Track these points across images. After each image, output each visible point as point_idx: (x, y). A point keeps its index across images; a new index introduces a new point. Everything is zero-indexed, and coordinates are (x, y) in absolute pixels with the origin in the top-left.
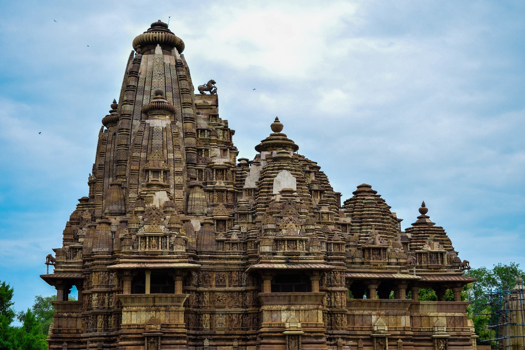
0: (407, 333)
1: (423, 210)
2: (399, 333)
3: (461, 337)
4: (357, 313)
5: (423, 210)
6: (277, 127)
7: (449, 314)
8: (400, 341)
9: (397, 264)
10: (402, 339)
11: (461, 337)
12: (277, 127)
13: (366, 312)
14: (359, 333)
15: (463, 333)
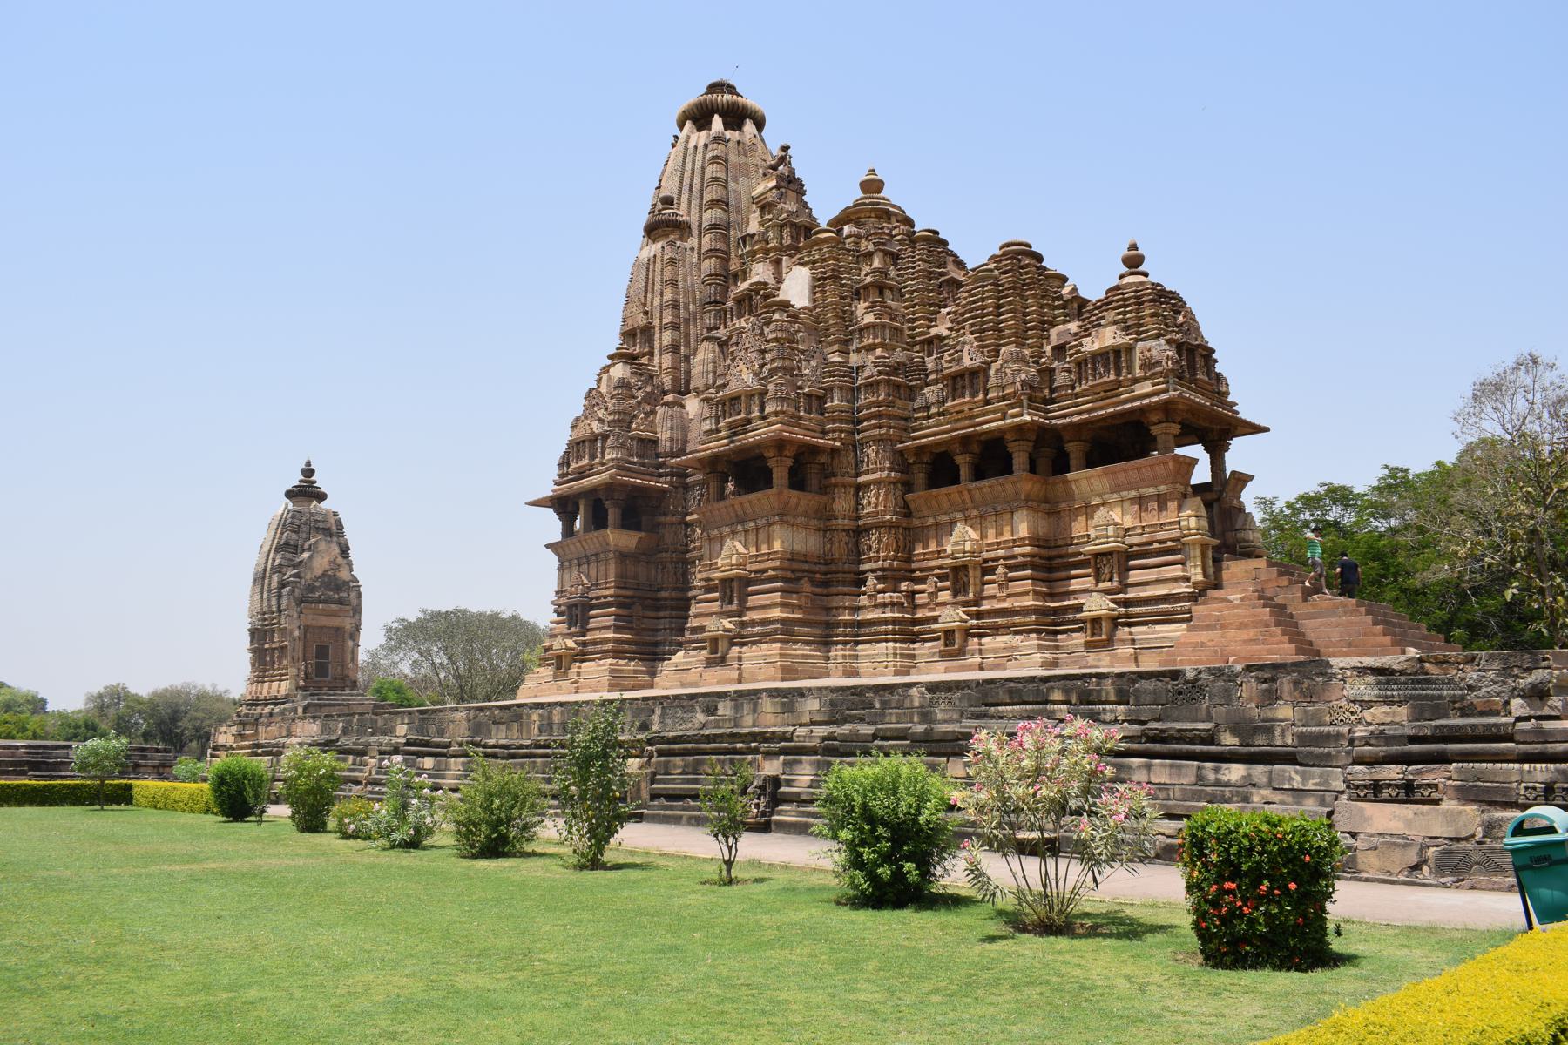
0: (1017, 550)
1: (1133, 262)
2: (1001, 553)
3: (1156, 545)
4: (931, 521)
5: (1133, 262)
6: (872, 186)
7: (1134, 493)
8: (1000, 570)
9: (1004, 399)
10: (1006, 566)
11: (1156, 545)
12: (872, 186)
13: (945, 518)
14: (932, 564)
15: (1162, 535)
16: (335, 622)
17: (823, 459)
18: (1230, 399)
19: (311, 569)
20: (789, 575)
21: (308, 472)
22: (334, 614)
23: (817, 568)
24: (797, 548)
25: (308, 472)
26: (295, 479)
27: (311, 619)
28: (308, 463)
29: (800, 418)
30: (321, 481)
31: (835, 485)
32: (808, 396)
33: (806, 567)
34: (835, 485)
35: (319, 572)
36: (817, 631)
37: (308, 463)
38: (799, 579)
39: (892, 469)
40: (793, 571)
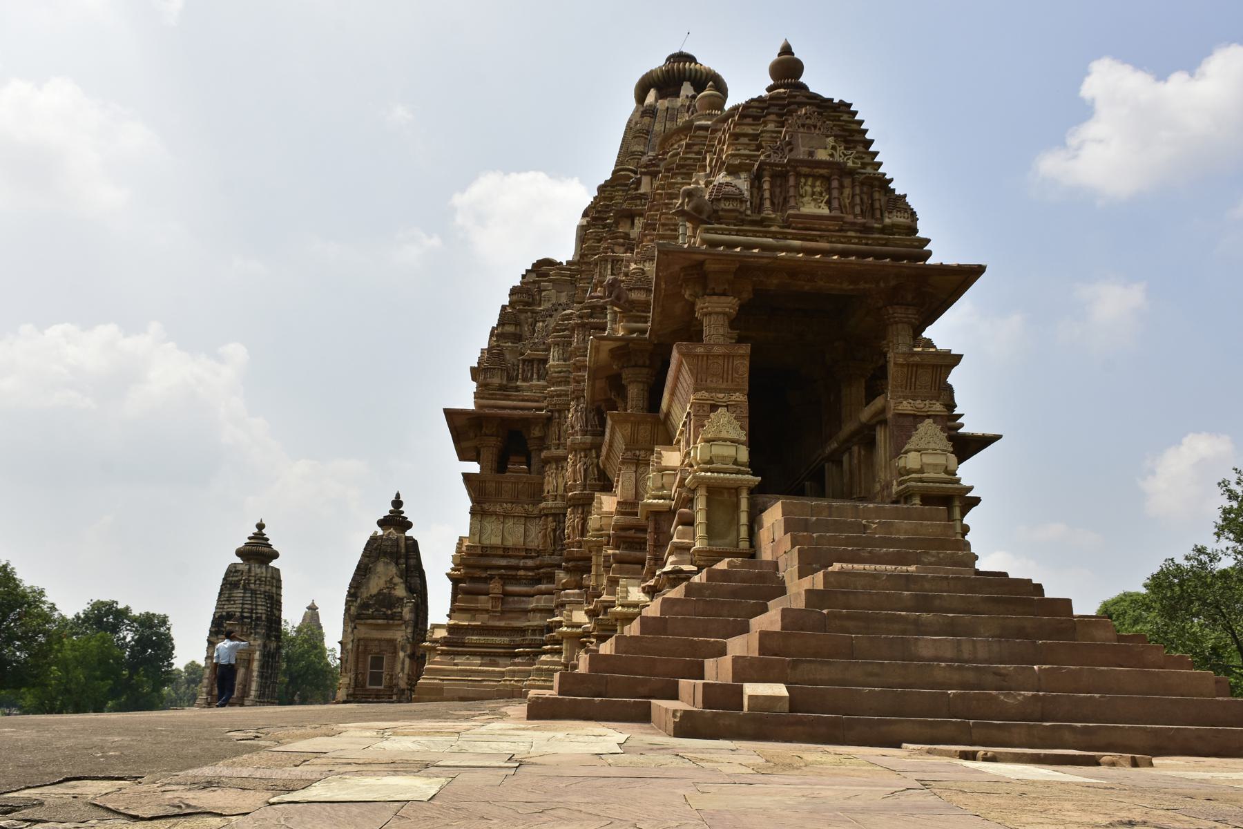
16: (388, 635)
17: (536, 432)
18: (921, 234)
19: (368, 588)
20: (478, 573)
21: (397, 503)
22: (387, 627)
23: (522, 563)
24: (496, 540)
25: (397, 503)
26: (386, 510)
27: (363, 632)
28: (398, 496)
29: (517, 389)
30: (408, 512)
31: (547, 462)
32: (531, 361)
33: (503, 562)
34: (547, 462)
35: (374, 591)
36: (506, 640)
37: (398, 496)
38: (491, 578)
39: (585, 433)
40: (487, 568)
